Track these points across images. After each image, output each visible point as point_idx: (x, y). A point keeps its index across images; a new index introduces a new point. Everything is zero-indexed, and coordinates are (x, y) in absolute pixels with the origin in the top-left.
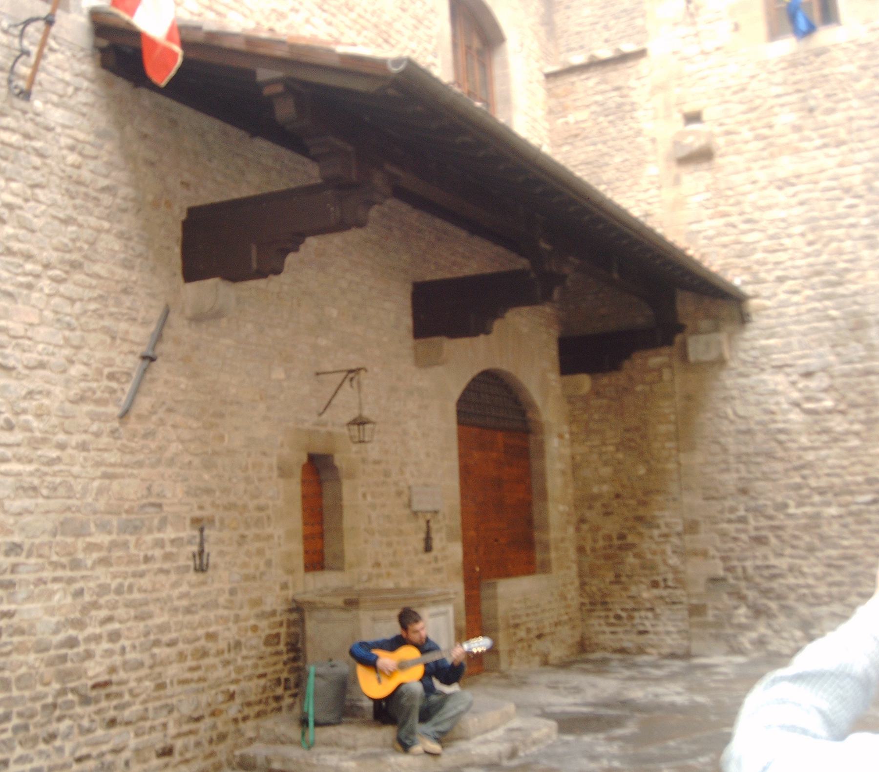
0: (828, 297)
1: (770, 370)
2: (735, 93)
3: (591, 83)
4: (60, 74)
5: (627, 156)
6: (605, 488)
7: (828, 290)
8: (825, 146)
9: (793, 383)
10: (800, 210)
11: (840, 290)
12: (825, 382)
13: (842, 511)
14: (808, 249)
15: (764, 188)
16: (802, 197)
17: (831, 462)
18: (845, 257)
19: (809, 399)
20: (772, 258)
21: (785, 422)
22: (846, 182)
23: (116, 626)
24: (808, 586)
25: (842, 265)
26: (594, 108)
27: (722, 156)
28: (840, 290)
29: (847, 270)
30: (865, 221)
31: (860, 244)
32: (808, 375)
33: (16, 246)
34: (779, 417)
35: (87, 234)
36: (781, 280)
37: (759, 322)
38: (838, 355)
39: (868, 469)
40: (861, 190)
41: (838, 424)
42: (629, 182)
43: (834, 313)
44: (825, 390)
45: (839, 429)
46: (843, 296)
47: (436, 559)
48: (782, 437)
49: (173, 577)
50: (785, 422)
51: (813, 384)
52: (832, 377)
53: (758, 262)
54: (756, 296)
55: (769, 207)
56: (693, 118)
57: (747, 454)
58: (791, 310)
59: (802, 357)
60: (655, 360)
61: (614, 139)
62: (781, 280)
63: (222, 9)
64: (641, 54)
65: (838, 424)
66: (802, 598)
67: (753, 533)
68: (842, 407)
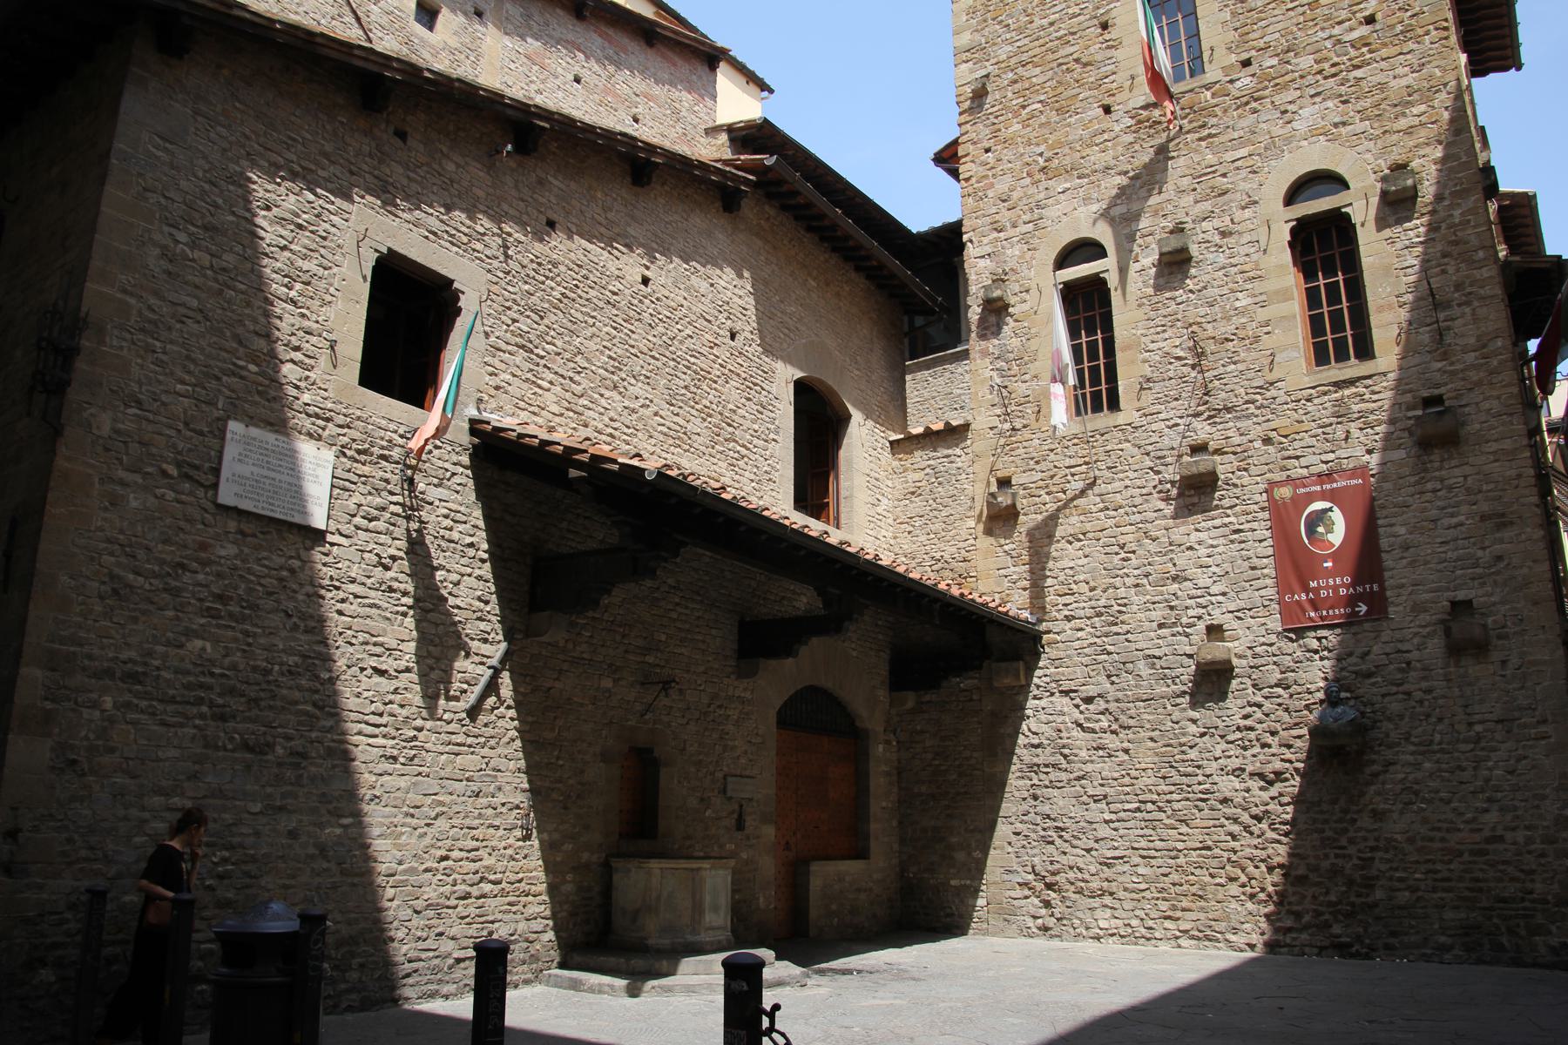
2: (1037, 463)
4: (440, 463)
6: (924, 789)
9: (1077, 706)
10: (1084, 561)
12: (1102, 705)
13: (1113, 817)
16: (1087, 551)
17: (1104, 773)
20: (1061, 600)
23: (450, 863)
24: (1083, 881)
26: (928, 470)
28: (1115, 629)
29: (1120, 612)
30: (1136, 572)
32: (1089, 700)
33: (395, 585)
35: (455, 577)
36: (1068, 618)
37: (1050, 652)
38: (1113, 683)
39: (1135, 781)
40: (1133, 546)
41: (1111, 741)
47: (748, 838)
48: (1066, 751)
49: (501, 832)
51: (1090, 707)
52: (1107, 702)
54: (1049, 632)
56: (1004, 483)
57: (1038, 766)
58: (1077, 644)
60: (967, 683)
63: (580, 409)
65: (1111, 741)
66: (1080, 892)
67: (1042, 833)
68: (1115, 727)
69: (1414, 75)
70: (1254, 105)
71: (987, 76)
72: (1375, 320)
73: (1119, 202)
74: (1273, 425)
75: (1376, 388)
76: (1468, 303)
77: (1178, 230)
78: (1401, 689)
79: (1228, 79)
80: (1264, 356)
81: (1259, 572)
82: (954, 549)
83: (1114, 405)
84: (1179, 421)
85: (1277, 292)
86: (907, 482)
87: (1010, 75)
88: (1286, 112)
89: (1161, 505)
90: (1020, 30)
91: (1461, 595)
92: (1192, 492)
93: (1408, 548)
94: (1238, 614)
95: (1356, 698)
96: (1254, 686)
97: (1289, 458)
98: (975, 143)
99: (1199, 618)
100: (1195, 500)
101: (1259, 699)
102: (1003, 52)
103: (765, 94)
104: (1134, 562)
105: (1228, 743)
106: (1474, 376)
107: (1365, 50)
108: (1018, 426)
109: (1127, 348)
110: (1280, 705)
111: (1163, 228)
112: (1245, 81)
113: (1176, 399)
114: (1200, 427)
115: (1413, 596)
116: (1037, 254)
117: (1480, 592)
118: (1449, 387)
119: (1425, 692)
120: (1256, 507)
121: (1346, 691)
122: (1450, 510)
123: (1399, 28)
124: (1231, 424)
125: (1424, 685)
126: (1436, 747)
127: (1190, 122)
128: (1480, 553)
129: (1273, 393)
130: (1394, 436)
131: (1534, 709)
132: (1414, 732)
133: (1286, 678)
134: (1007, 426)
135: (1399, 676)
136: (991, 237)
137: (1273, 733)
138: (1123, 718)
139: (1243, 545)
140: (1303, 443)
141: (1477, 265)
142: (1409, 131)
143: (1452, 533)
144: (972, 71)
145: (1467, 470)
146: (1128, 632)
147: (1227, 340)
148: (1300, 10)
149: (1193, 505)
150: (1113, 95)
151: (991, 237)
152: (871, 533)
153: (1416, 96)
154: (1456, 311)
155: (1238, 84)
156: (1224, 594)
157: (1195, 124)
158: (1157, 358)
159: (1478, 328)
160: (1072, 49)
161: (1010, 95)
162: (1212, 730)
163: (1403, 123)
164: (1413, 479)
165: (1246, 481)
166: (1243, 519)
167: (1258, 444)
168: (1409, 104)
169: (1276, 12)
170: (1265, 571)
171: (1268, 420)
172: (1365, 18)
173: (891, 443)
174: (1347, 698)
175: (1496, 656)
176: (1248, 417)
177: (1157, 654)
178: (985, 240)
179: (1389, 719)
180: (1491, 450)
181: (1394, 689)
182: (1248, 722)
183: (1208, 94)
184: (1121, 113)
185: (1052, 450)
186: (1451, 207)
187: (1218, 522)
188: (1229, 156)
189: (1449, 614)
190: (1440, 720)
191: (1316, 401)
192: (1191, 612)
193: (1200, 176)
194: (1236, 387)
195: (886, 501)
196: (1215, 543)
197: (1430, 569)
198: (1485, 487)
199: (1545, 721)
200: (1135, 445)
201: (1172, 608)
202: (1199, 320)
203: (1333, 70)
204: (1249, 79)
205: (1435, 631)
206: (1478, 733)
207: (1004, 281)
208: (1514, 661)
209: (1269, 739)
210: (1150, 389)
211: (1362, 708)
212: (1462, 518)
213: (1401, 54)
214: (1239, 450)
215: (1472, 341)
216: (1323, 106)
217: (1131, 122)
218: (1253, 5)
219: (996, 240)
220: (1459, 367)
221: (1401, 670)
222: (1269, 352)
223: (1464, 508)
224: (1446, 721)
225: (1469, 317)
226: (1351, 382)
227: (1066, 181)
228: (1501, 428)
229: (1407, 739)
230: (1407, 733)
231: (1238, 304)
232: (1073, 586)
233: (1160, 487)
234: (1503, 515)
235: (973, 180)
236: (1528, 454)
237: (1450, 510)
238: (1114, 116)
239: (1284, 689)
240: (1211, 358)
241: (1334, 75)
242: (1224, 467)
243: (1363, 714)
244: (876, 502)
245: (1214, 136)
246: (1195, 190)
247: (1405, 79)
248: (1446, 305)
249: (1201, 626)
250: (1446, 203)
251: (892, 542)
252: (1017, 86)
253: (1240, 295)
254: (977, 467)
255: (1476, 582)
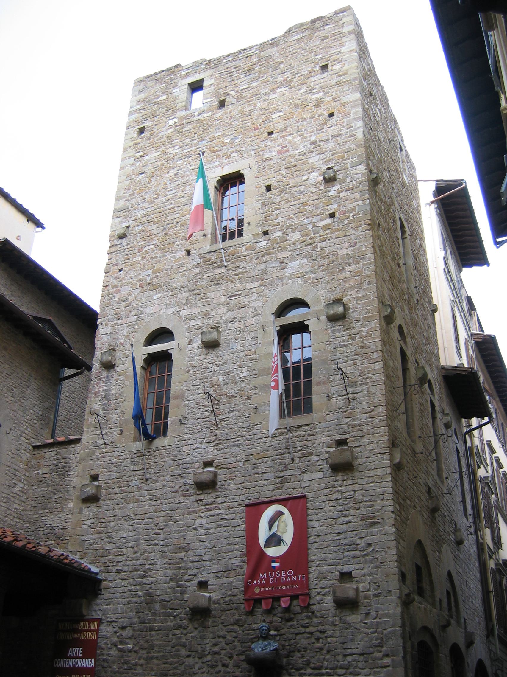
0: (140, 584)
1: (105, 624)
3: (53, 454)
5: (61, 495)
7: (140, 580)
8: (150, 499)
10: (134, 533)
11: (145, 580)
14: (134, 556)
15: (120, 519)
18: (149, 562)
19: (121, 642)
21: (108, 655)
22: (156, 520)
25: (148, 566)
27: (103, 500)
28: (145, 580)
29: (149, 569)
31: (158, 556)
32: (123, 628)
34: (105, 652)
36: (119, 571)
37: (105, 594)
40: (161, 525)
42: (59, 510)
43: (140, 593)
44: (130, 638)
45: (133, 662)
46: (146, 584)
48: (105, 664)
50: (108, 655)
51: (125, 633)
52: (134, 630)
53: (109, 561)
54: (105, 580)
55: (119, 531)
56: (95, 478)
59: (121, 618)
61: (57, 485)
62: (119, 571)
64: (78, 441)
65: (133, 659)
68: (136, 648)
69: (352, 248)
70: (266, 257)
71: (128, 227)
72: (315, 388)
73: (186, 308)
74: (252, 451)
75: (311, 433)
76: (366, 384)
77: (216, 328)
78: (308, 630)
79: (255, 241)
80: (251, 408)
81: (231, 547)
82: (58, 521)
83: (165, 433)
84: (198, 445)
85: (263, 369)
86: (38, 474)
87: (140, 228)
88: (282, 263)
89: (181, 499)
90: (151, 202)
91: (346, 569)
92: (201, 492)
93: (319, 536)
94: (218, 575)
95: (281, 635)
96: (222, 623)
97: (258, 473)
98: (114, 265)
99: (195, 575)
100: (202, 497)
101: (222, 633)
102: (140, 213)
103: (40, 229)
104: (162, 536)
105: (203, 663)
106: (365, 428)
107: (328, 231)
108: (108, 440)
109: (176, 397)
110: (236, 637)
111: (207, 325)
112: (263, 244)
113: (199, 432)
114: (210, 450)
115: (319, 568)
116: (136, 335)
117: (357, 567)
118: (351, 434)
119: (321, 632)
120: (236, 504)
121: (276, 629)
122: (344, 512)
123: (346, 221)
124: (228, 450)
125: (320, 628)
126: (324, 671)
127: (232, 263)
128: (359, 541)
129: (254, 431)
130: (318, 463)
131: (382, 647)
132: (313, 660)
133: (240, 620)
134: (101, 442)
135: (307, 621)
136: (113, 323)
137: (230, 657)
138: (142, 642)
139: (225, 528)
140: (267, 465)
141: (373, 361)
142: (345, 280)
143: (345, 527)
144: (121, 223)
145: (356, 487)
146: (152, 583)
147: (233, 396)
148: (298, 206)
149: (201, 500)
150: (193, 244)
151: (113, 323)
152: (4, 505)
153: (351, 261)
154: (359, 389)
155: (260, 245)
156: (211, 560)
157: (234, 265)
158: (193, 405)
159: (370, 399)
160: (176, 216)
161: (138, 239)
162: (193, 654)
163: (342, 275)
164: (326, 491)
165: (232, 487)
166: (227, 511)
167: (241, 463)
168: (349, 264)
169: (285, 206)
170: (237, 547)
171: (249, 449)
172: (330, 214)
173: (34, 447)
174: (276, 635)
175: (363, 610)
176: (238, 446)
177: (167, 599)
178: (110, 324)
179: (299, 651)
180: (371, 475)
181: (303, 630)
182: (216, 649)
183: (244, 248)
184: (195, 255)
185: (125, 459)
186: (363, 325)
187: (212, 513)
188: (249, 286)
189: (339, 581)
190: (328, 652)
191: (278, 438)
192: (190, 572)
193: (231, 297)
194: (233, 426)
195: (22, 485)
196: (209, 526)
197: (330, 550)
198: (365, 499)
199: (387, 655)
200: (173, 460)
201: (180, 568)
202: (218, 383)
203: (311, 241)
204: (266, 242)
205: (329, 591)
206: (349, 662)
207: (115, 350)
208: (373, 613)
209: (227, 660)
210: (185, 424)
211: (283, 642)
212: (350, 518)
213: (345, 236)
214: (231, 466)
215: (366, 406)
216: (302, 261)
217: (199, 260)
218: (274, 201)
219: (116, 324)
220: (358, 422)
221: (308, 617)
222: (254, 406)
223: (353, 512)
224: (332, 653)
225: (365, 392)
226: (298, 427)
227: (159, 293)
228: (377, 462)
229: (308, 665)
230: (309, 660)
231: (242, 375)
232: (124, 550)
233: (183, 487)
234: (373, 517)
235: (110, 286)
236: (390, 479)
237: (344, 512)
238: (191, 257)
239: (240, 626)
240: (222, 407)
241: (311, 244)
242: (222, 475)
243: (283, 646)
244: (12, 484)
245: (242, 273)
246: (227, 304)
247: (347, 250)
248: (353, 384)
249: (195, 582)
250: (360, 323)
251: (22, 513)
252: (143, 234)
253: (244, 370)
254: (80, 467)
255: (355, 559)
